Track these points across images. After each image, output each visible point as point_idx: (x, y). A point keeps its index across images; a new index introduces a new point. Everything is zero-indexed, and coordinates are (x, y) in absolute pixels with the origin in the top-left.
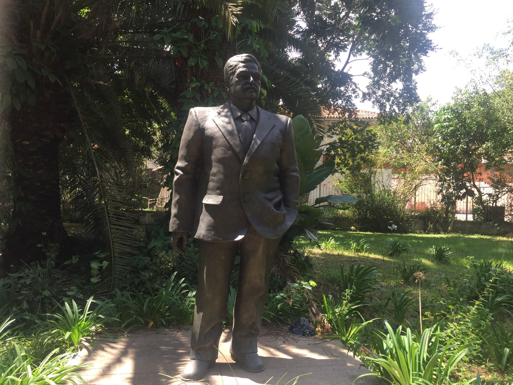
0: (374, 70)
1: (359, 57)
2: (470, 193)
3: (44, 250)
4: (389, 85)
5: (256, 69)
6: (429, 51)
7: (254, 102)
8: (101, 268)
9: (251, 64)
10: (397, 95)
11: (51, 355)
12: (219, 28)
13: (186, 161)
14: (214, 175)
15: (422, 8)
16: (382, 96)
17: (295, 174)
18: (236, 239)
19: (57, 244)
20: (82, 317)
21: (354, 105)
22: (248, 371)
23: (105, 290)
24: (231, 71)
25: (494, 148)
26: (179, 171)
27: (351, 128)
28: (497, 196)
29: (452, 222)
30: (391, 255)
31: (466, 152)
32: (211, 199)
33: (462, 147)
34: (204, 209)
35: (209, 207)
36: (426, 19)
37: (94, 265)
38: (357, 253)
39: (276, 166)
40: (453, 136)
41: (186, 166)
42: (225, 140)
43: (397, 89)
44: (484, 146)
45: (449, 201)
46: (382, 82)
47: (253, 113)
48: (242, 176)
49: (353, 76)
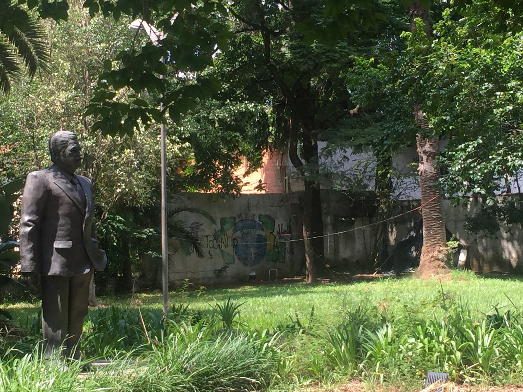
14: (61, 226)
18: (85, 273)
34: (55, 253)
35: (58, 250)
41: (37, 219)
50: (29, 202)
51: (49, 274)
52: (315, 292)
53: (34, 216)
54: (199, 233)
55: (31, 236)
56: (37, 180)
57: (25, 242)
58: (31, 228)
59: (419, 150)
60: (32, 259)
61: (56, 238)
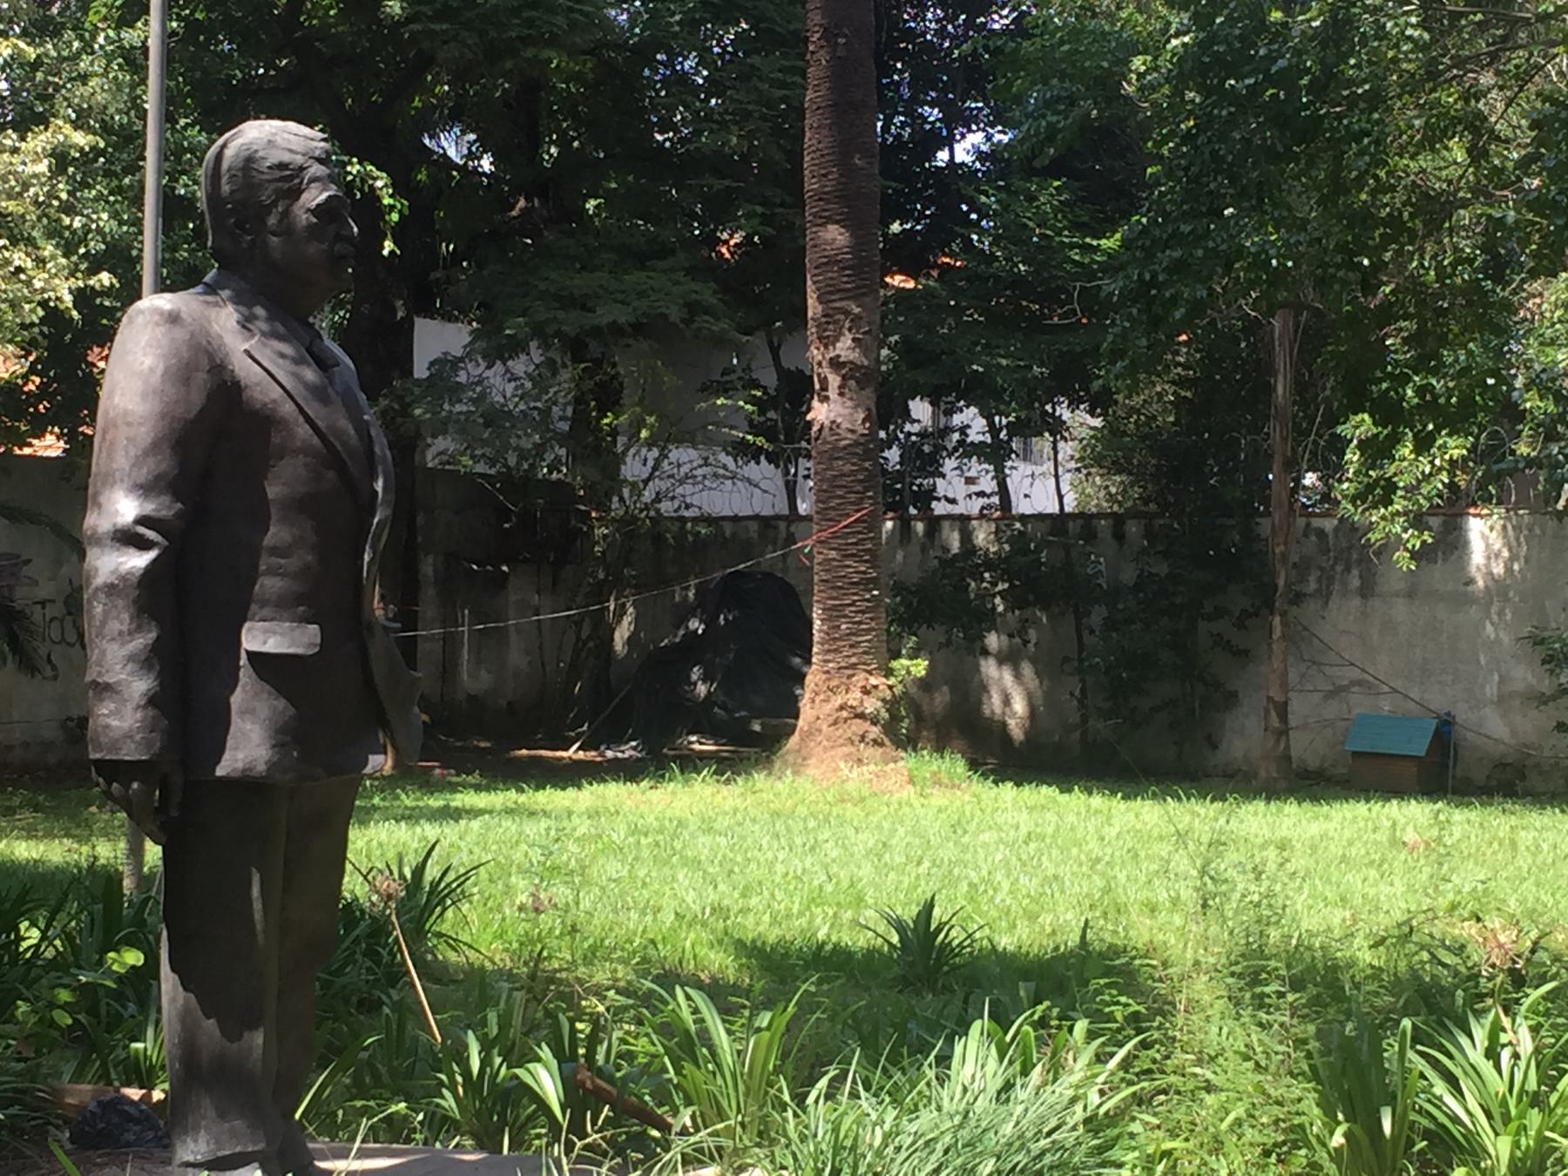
13: (177, 497)
14: (275, 551)
32: (261, 637)
34: (246, 674)
50: (145, 434)
51: (220, 772)
52: (474, 813)
53: (166, 499)
54: (20, 592)
55: (149, 594)
56: (180, 334)
57: (121, 621)
58: (152, 555)
59: (815, 353)
60: (152, 701)
61: (254, 607)
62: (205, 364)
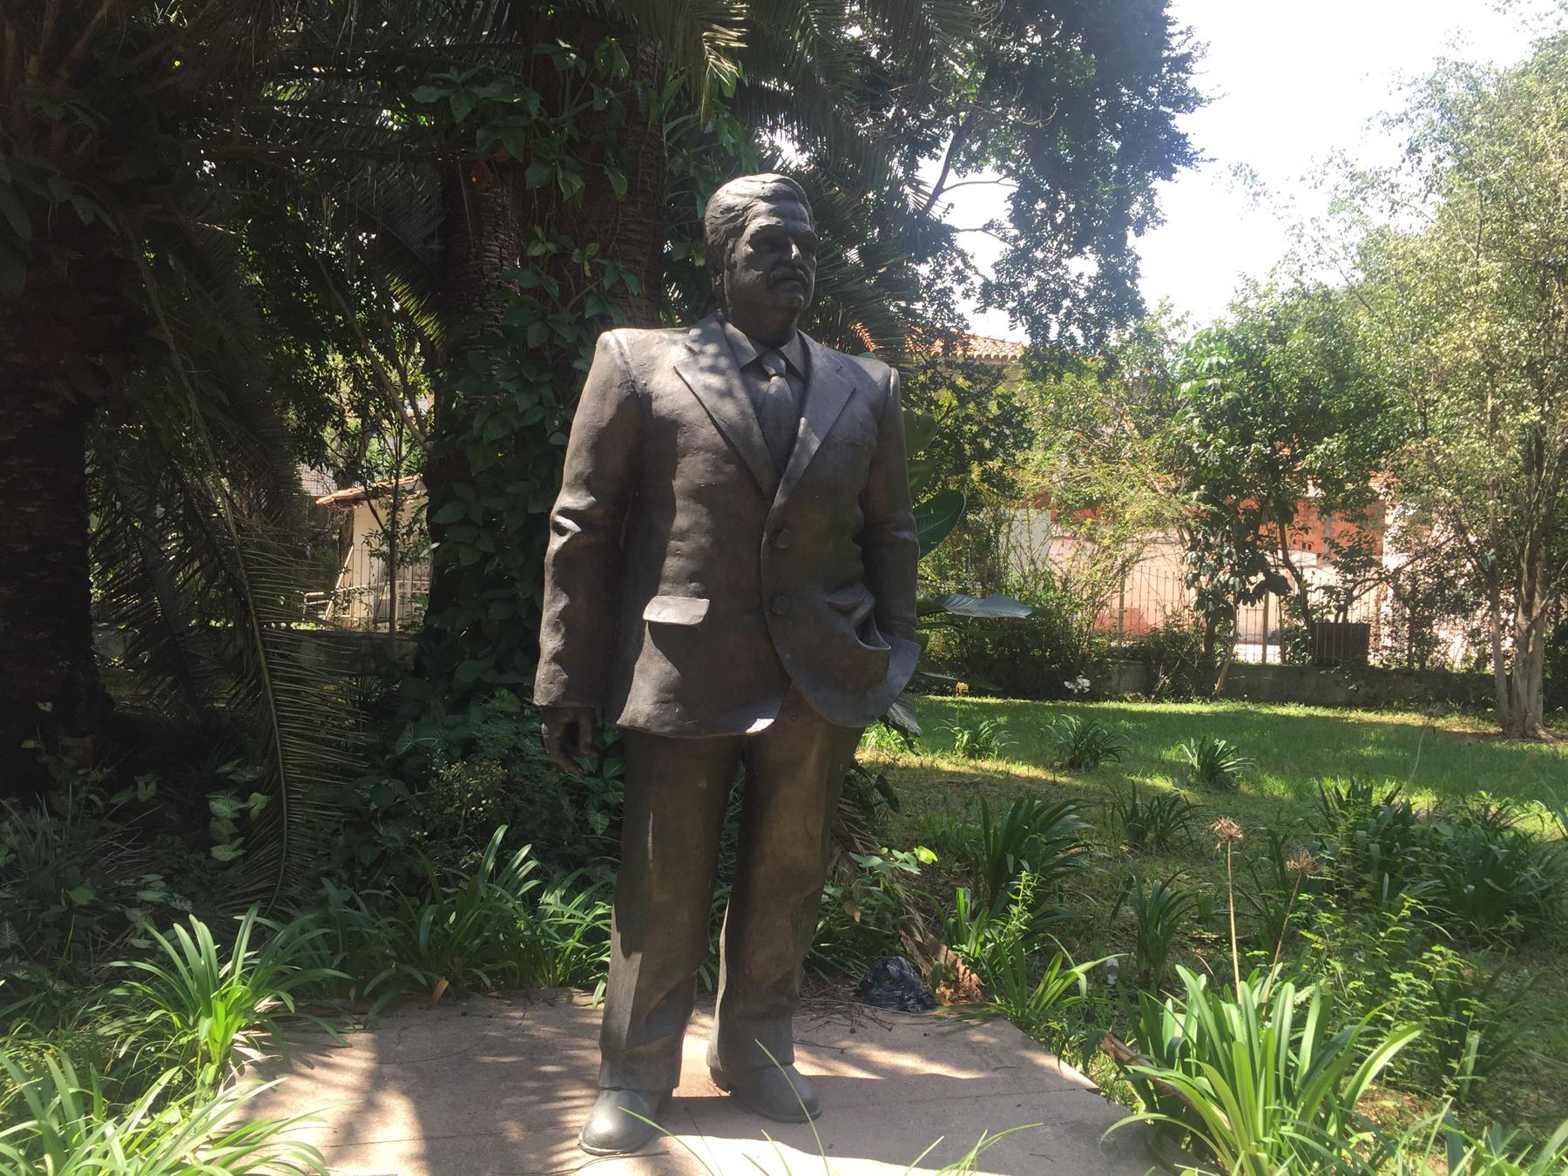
0: (1020, 216)
1: (972, 176)
2: (1278, 586)
3: (44, 759)
4: (1058, 264)
5: (804, 220)
6: (1179, 167)
7: (796, 321)
8: (245, 813)
9: (792, 205)
10: (1082, 294)
11: (156, 1090)
12: (616, 78)
14: (683, 535)
15: (1162, 42)
16: (1038, 295)
17: (906, 535)
18: (751, 730)
19: (88, 740)
20: (229, 966)
21: (961, 317)
22: (776, 1120)
23: (262, 885)
24: (731, 225)
25: (1351, 453)
26: (568, 523)
27: (953, 387)
28: (1349, 592)
29: (1225, 668)
30: (1073, 766)
31: (1269, 467)
32: (671, 609)
33: (1259, 452)
34: (648, 637)
35: (663, 632)
36: (1170, 72)
37: (222, 806)
38: (972, 762)
39: (858, 511)
40: (1233, 419)
41: (592, 507)
42: (715, 431)
43: (1081, 275)
44: (1320, 448)
45: (1217, 610)
46: (1039, 254)
47: (791, 350)
48: (770, 542)
49: (958, 231)
62: (618, 379)
